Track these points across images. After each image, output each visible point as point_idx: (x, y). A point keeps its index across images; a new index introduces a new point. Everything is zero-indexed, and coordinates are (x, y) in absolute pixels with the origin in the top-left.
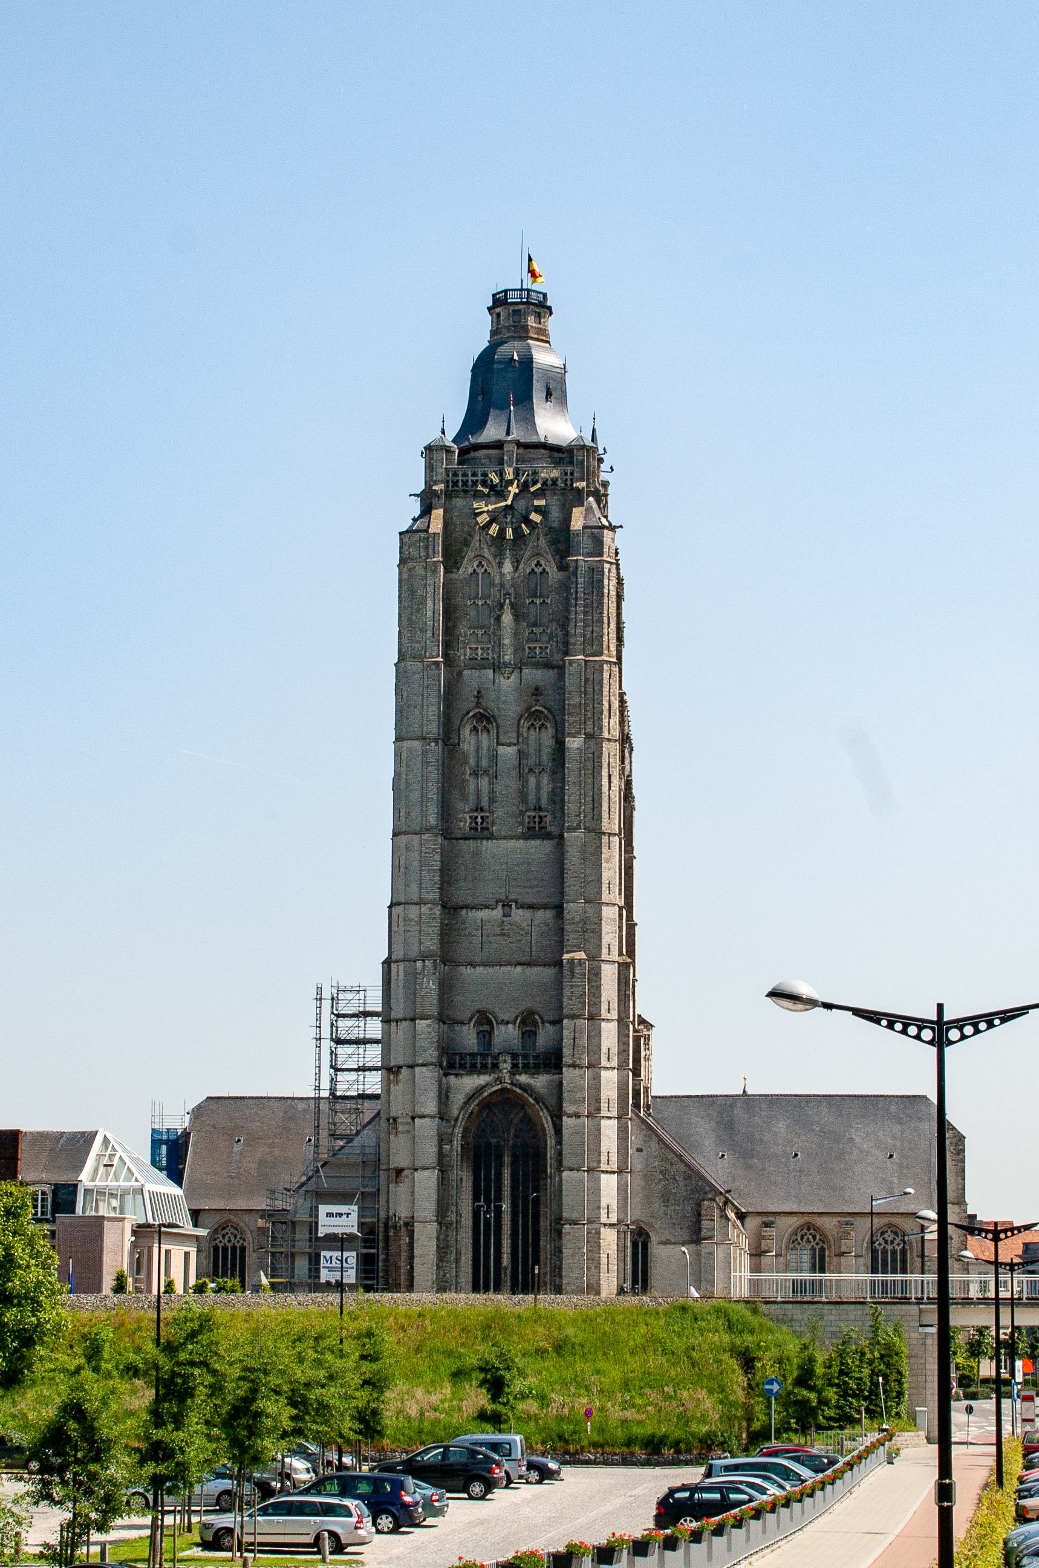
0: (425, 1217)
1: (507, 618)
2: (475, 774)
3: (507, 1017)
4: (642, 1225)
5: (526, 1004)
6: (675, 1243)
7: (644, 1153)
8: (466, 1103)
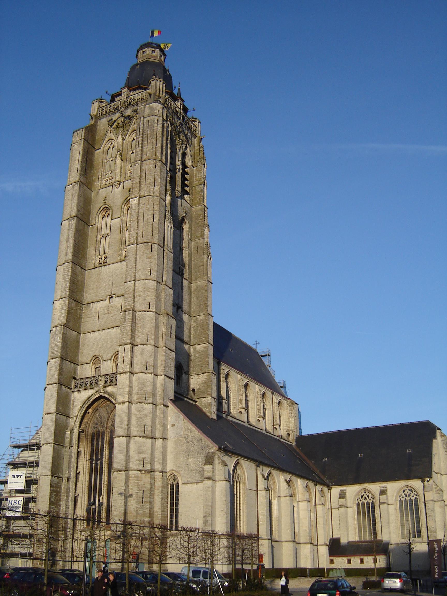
0: (46, 473)
3: (106, 358)
4: (174, 472)
8: (81, 407)
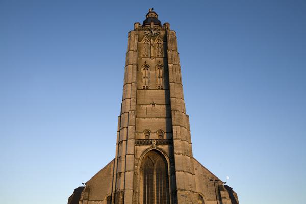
1: (152, 49)
2: (145, 77)
5: (160, 128)
6: (212, 200)
7: (198, 170)
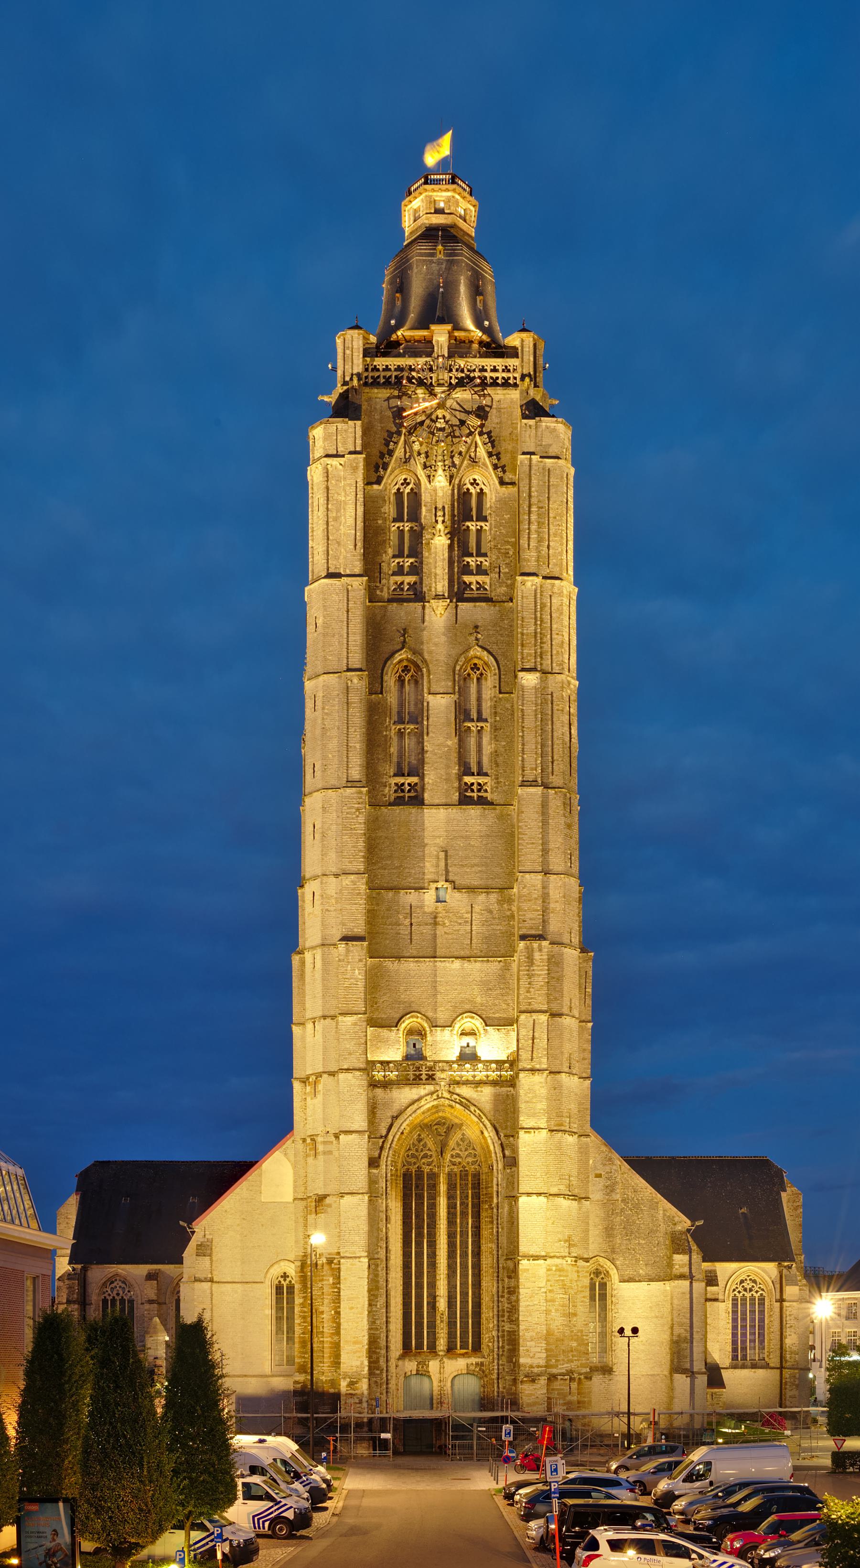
0: (354, 1253)
